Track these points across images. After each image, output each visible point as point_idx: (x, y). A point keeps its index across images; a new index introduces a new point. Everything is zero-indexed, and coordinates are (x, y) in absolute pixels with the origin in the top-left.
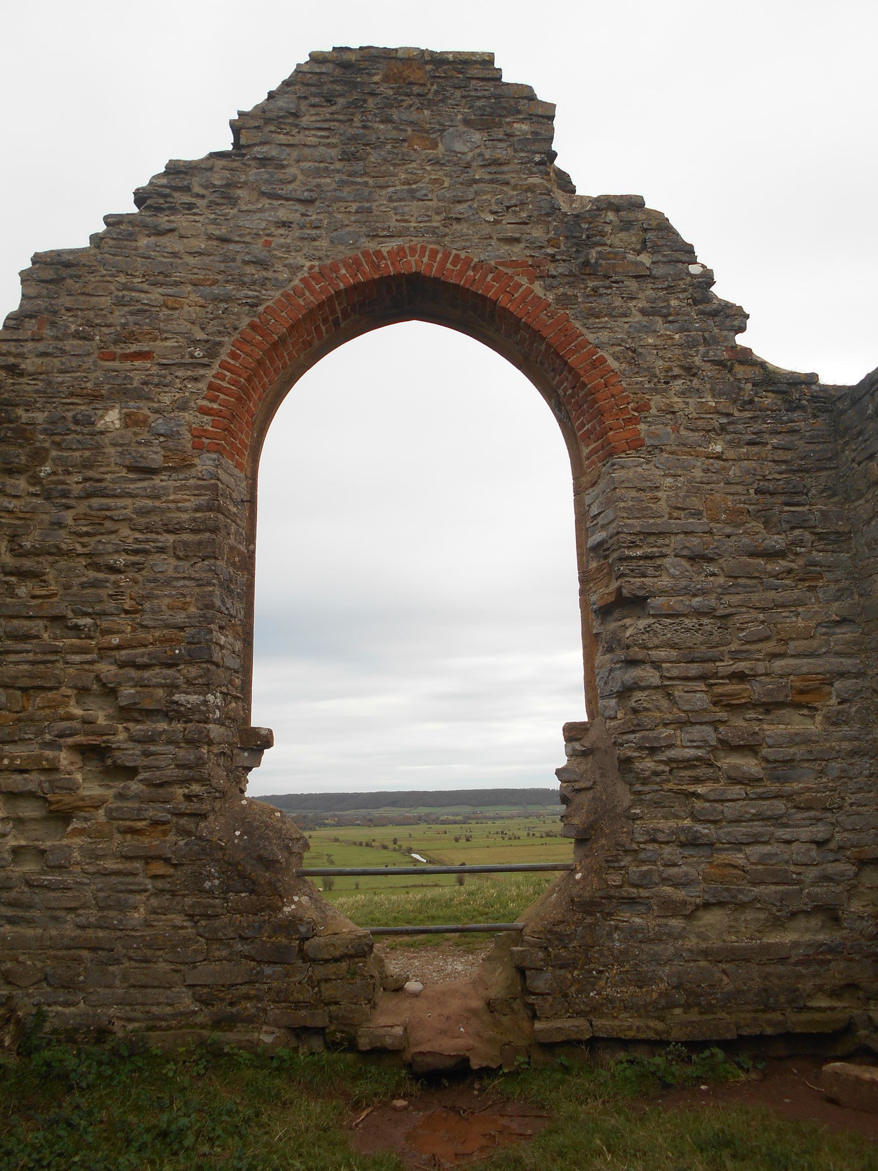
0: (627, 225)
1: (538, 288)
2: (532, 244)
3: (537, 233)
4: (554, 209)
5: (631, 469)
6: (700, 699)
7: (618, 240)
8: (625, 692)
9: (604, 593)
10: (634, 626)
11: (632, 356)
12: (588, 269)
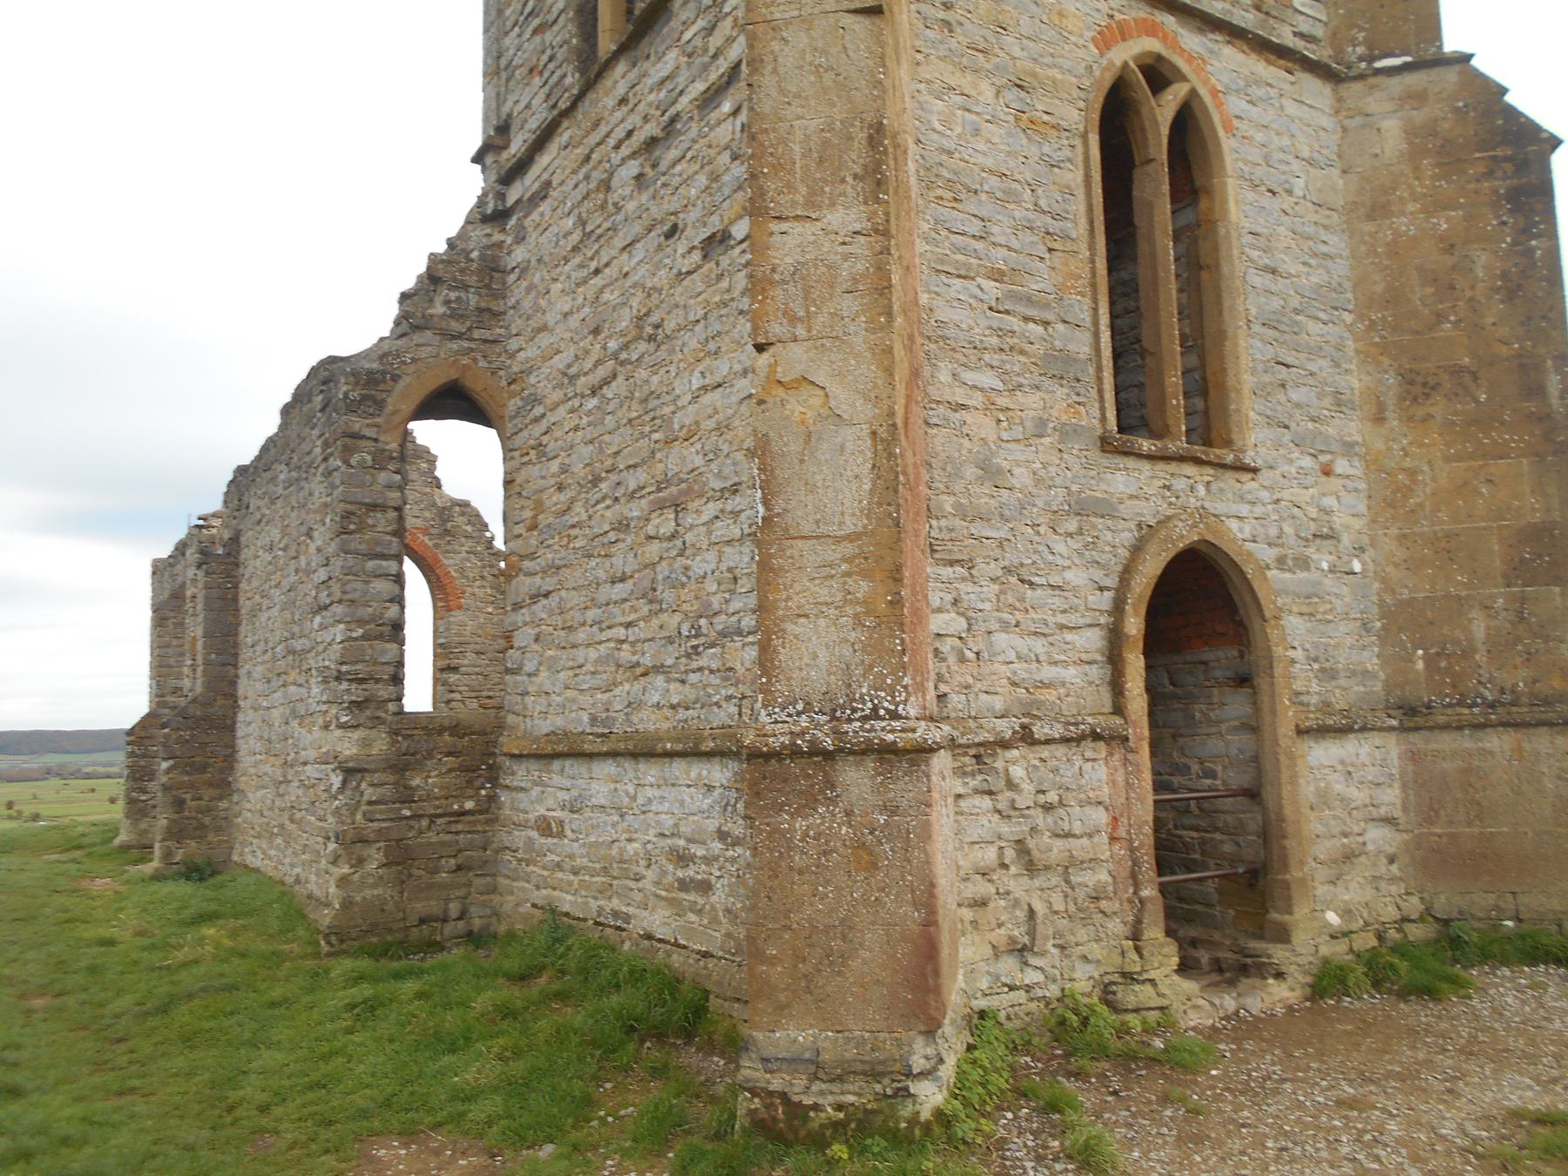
0: (463, 514)
1: (426, 539)
2: (425, 519)
3: (427, 514)
4: (434, 504)
5: (458, 616)
6: (475, 705)
7: (460, 520)
8: (448, 702)
9: (443, 663)
10: (453, 678)
11: (462, 570)
12: (447, 532)
